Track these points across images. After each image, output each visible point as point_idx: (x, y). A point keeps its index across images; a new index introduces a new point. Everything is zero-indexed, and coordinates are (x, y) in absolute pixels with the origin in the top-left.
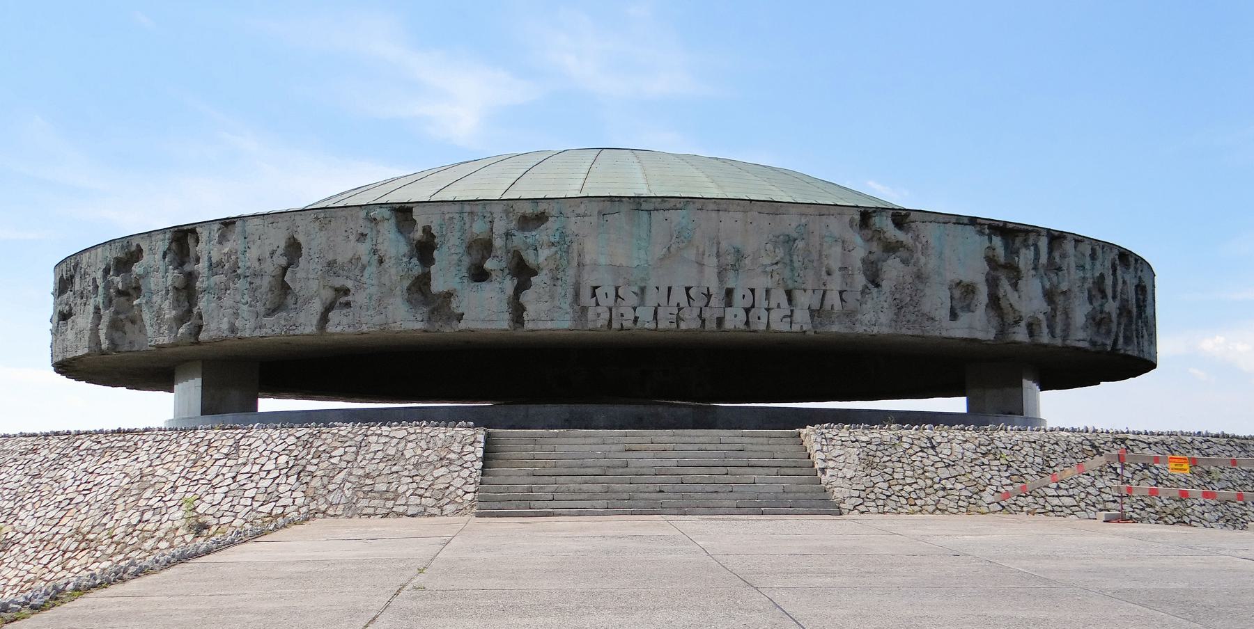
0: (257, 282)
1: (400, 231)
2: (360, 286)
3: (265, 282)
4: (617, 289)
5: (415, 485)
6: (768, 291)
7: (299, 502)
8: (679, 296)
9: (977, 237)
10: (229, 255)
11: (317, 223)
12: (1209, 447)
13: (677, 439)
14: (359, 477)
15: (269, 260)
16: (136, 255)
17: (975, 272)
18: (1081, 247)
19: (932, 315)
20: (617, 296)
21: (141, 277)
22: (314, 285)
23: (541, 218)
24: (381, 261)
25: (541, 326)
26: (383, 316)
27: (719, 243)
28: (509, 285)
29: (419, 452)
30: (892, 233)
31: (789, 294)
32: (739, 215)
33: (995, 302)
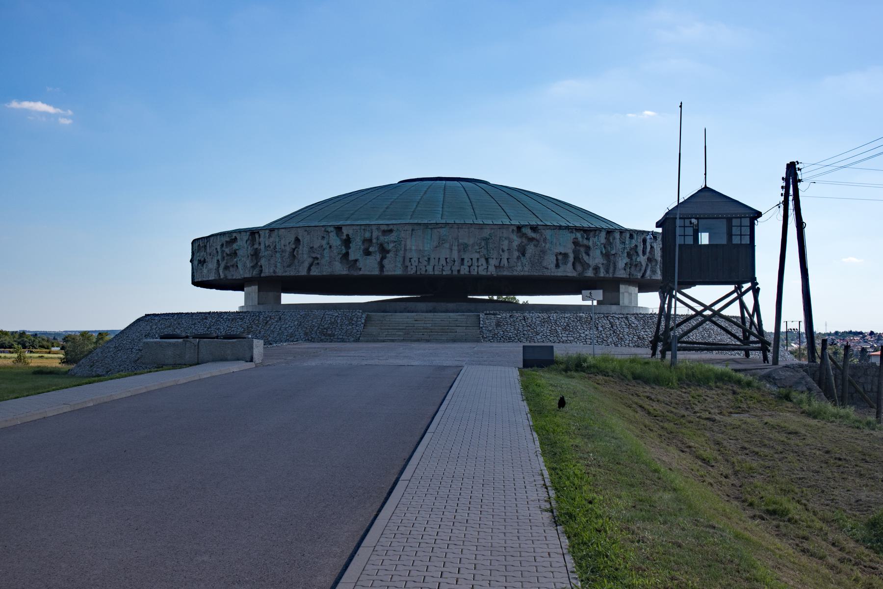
0: (284, 254)
1: (338, 236)
2: (323, 256)
3: (287, 254)
4: (419, 259)
5: (340, 332)
6: (478, 259)
7: (302, 337)
8: (443, 262)
9: (569, 235)
10: (273, 242)
11: (306, 232)
12: (651, 319)
13: (434, 317)
14: (322, 329)
15: (288, 246)
16: (235, 240)
17: (569, 249)
18: (624, 235)
19: (547, 267)
20: (419, 262)
21: (237, 250)
22: (305, 256)
23: (391, 231)
24: (330, 247)
25: (390, 273)
26: (331, 269)
27: (458, 241)
28: (378, 257)
29: (342, 321)
30: (531, 234)
31: (487, 260)
32: (466, 230)
33: (577, 259)
